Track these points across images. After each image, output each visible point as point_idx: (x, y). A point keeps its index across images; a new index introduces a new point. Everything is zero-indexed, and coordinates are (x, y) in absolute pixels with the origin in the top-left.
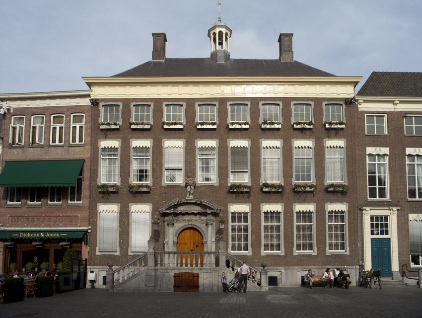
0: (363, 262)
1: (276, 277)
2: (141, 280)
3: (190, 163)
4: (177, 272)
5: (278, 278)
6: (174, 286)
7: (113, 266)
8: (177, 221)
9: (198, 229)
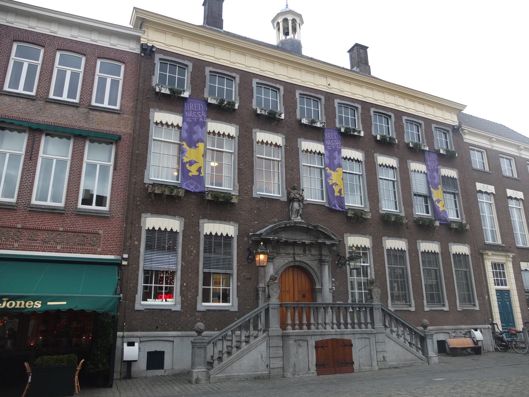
0: (493, 320)
2: (260, 357)
3: (292, 170)
4: (319, 338)
6: (317, 365)
7: (204, 331)
8: (278, 254)
9: (308, 268)
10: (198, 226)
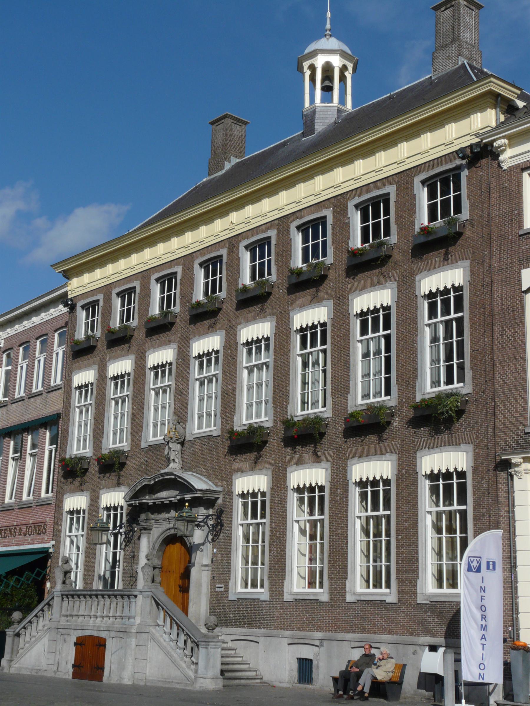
1: (311, 660)
4: (80, 633)
5: (315, 663)
10: (99, 499)
